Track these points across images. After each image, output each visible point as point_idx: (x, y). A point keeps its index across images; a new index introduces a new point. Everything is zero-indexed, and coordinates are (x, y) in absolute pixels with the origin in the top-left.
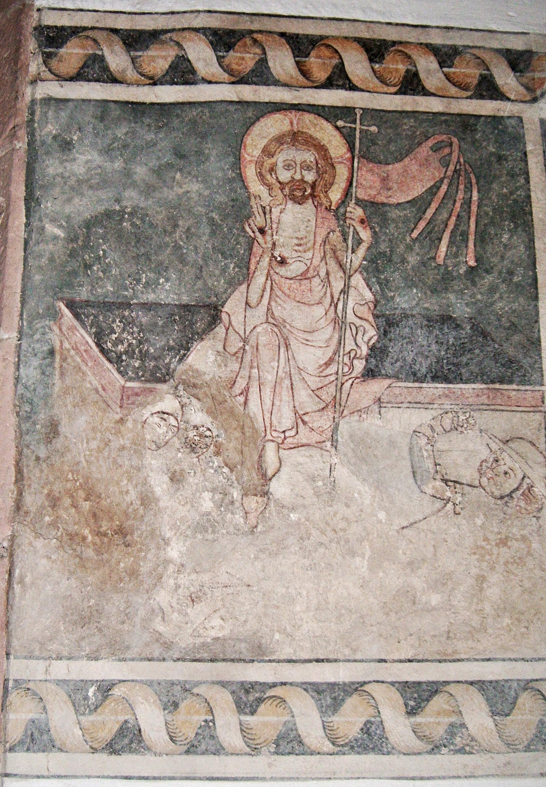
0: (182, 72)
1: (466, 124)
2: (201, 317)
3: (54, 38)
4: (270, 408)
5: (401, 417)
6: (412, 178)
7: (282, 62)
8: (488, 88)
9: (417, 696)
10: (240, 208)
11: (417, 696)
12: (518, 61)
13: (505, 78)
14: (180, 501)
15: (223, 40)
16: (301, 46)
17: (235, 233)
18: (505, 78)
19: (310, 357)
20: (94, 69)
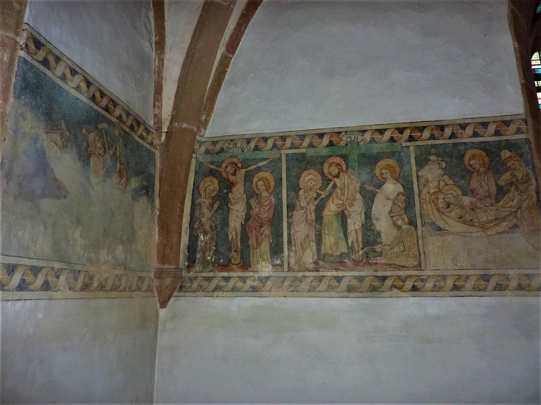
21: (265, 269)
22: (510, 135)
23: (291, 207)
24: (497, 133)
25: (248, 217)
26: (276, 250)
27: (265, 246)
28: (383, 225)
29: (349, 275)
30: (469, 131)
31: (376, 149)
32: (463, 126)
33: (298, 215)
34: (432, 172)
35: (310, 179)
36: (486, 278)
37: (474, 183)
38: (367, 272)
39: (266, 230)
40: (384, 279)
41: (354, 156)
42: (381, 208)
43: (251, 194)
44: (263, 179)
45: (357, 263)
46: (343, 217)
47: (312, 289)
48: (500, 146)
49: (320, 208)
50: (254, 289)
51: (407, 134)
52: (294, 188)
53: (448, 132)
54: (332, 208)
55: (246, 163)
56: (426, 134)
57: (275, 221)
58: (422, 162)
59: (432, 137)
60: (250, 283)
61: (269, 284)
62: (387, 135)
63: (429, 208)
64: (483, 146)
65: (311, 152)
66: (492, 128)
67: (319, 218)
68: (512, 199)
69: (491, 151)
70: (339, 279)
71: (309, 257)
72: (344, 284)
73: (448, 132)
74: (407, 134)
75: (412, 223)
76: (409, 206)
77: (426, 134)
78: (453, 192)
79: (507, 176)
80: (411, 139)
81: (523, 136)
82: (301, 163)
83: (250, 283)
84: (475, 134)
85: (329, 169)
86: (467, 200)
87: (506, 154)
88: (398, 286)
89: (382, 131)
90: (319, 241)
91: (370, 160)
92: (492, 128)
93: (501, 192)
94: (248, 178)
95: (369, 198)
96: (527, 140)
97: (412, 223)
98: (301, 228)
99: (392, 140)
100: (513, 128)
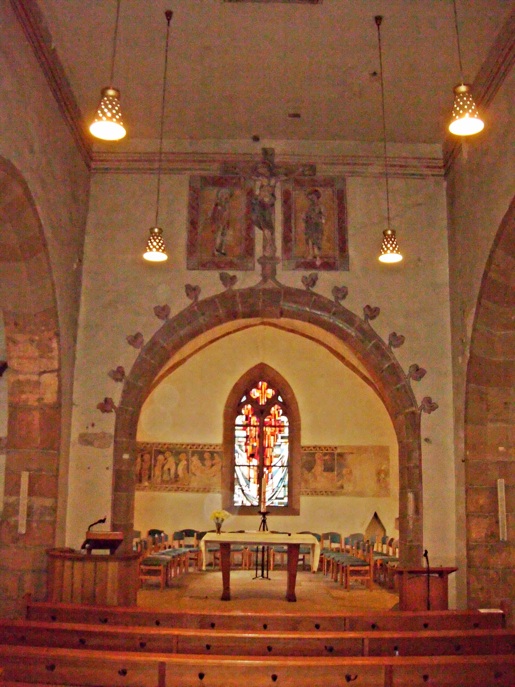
0: (311, 450)
1: (331, 453)
2: (312, 468)
3: (302, 447)
5: (325, 474)
6: (327, 457)
7: (318, 449)
8: (333, 450)
9: (326, 492)
10: (315, 460)
11: (326, 492)
12: (336, 448)
13: (334, 449)
15: (314, 447)
16: (320, 448)
18: (334, 449)
19: (320, 470)
20: (305, 450)
21: (146, 484)
22: (217, 449)
23: (155, 466)
24: (214, 448)
27: (147, 477)
28: (180, 472)
29: (170, 486)
30: (206, 447)
32: (205, 445)
33: (156, 468)
34: (195, 460)
35: (161, 457)
36: (205, 489)
37: (206, 463)
38: (175, 486)
40: (178, 488)
41: (174, 451)
42: (181, 468)
43: (143, 461)
44: (147, 457)
45: (172, 483)
46: (169, 469)
47: (159, 490)
48: (215, 452)
49: (163, 467)
51: (189, 447)
52: (156, 460)
53: (201, 447)
54: (166, 468)
56: (195, 447)
57: (150, 470)
58: (193, 455)
59: (196, 448)
60: (141, 488)
61: (147, 488)
62: (184, 447)
66: (213, 447)
69: (212, 453)
70: (167, 487)
72: (168, 489)
73: (201, 447)
74: (189, 447)
75: (188, 472)
77: (195, 447)
79: (215, 461)
80: (191, 448)
81: (220, 450)
83: (141, 488)
84: (208, 448)
89: (183, 445)
92: (213, 447)
93: (213, 465)
94: (142, 456)
95: (177, 465)
96: (221, 452)
97: (188, 472)
98: (157, 472)
99: (185, 448)
100: (218, 447)
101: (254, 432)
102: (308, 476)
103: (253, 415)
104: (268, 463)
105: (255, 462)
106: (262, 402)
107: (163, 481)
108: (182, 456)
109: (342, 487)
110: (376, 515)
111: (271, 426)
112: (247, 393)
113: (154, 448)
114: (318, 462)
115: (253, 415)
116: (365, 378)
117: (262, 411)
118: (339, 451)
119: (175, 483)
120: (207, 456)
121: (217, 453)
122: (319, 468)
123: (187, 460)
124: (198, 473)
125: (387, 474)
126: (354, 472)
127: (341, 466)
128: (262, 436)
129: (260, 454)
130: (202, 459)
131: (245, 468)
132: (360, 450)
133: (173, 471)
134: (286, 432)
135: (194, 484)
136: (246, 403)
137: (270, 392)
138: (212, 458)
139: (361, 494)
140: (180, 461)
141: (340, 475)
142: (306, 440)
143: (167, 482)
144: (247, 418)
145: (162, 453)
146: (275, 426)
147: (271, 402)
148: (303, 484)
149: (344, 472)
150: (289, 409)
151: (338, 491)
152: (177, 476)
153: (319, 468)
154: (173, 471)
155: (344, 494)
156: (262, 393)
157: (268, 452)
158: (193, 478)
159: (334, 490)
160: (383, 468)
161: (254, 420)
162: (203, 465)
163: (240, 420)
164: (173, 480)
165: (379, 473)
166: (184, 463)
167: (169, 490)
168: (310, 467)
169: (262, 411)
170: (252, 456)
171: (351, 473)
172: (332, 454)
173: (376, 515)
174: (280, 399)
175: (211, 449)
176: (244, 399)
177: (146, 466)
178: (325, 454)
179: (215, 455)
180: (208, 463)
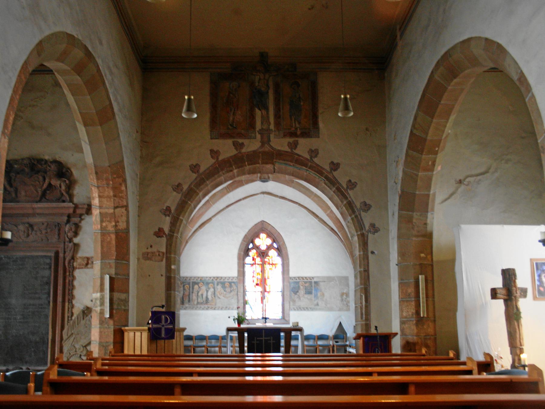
2: (298, 292)
4: (301, 296)
5: (306, 296)
6: (307, 285)
12: (313, 278)
14: (297, 300)
16: (302, 278)
17: (299, 287)
21: (187, 305)
22: (234, 280)
25: (184, 294)
26: (189, 301)
27: (187, 300)
28: (210, 297)
29: (202, 306)
31: (209, 281)
33: (194, 294)
34: (219, 287)
35: (196, 287)
37: (227, 289)
38: (206, 306)
39: (187, 297)
42: (210, 294)
43: (184, 289)
44: (187, 286)
46: (202, 295)
48: (232, 282)
49: (198, 293)
50: (185, 309)
52: (193, 289)
54: (200, 294)
55: (183, 283)
57: (189, 295)
58: (218, 285)
63: (218, 294)
64: (229, 282)
65: (197, 281)
67: (198, 295)
68: (232, 293)
69: (230, 283)
71: (196, 303)
76: (214, 293)
78: (222, 291)
82: (195, 283)
85: (200, 285)
86: (225, 293)
87: (233, 284)
88: (212, 308)
90: (197, 299)
91: (208, 284)
93: (231, 291)
94: (184, 286)
95: (207, 291)
101: (258, 269)
102: (295, 297)
103: (257, 257)
104: (267, 290)
105: (260, 289)
106: (263, 248)
107: (198, 303)
108: (210, 285)
109: (318, 305)
110: (340, 323)
111: (269, 264)
112: (253, 242)
113: (191, 281)
114: (301, 287)
115: (257, 257)
116: (332, 229)
117: (263, 254)
118: (315, 280)
119: (206, 303)
120: (227, 285)
121: (234, 282)
122: (302, 292)
123: (214, 288)
124: (221, 297)
125: (347, 295)
126: (326, 294)
127: (316, 290)
128: (263, 271)
129: (262, 283)
130: (224, 287)
131: (252, 293)
132: (330, 279)
133: (204, 296)
134: (279, 268)
135: (219, 305)
136: (253, 248)
137: (269, 241)
138: (231, 286)
139: (331, 309)
140: (209, 289)
141: (316, 296)
142: (293, 273)
143: (202, 303)
144: (253, 259)
145: (197, 283)
146: (272, 264)
147: (269, 248)
148: (291, 303)
149: (319, 294)
150: (280, 251)
151: (315, 307)
152: (207, 298)
153: (302, 292)
154: (204, 296)
155: (320, 310)
156: (263, 241)
157: (268, 281)
158: (218, 300)
159: (313, 306)
160: (345, 292)
161: (258, 260)
162: (225, 291)
163: (248, 260)
164: (205, 302)
165: (342, 294)
166: (212, 290)
167: (203, 309)
168: (295, 291)
169: (263, 254)
170: (257, 284)
171: (323, 295)
172: (311, 283)
173: (340, 323)
174: (275, 245)
175: (230, 281)
176: (251, 246)
177: (187, 293)
178: (306, 283)
179: (233, 284)
180: (228, 290)
